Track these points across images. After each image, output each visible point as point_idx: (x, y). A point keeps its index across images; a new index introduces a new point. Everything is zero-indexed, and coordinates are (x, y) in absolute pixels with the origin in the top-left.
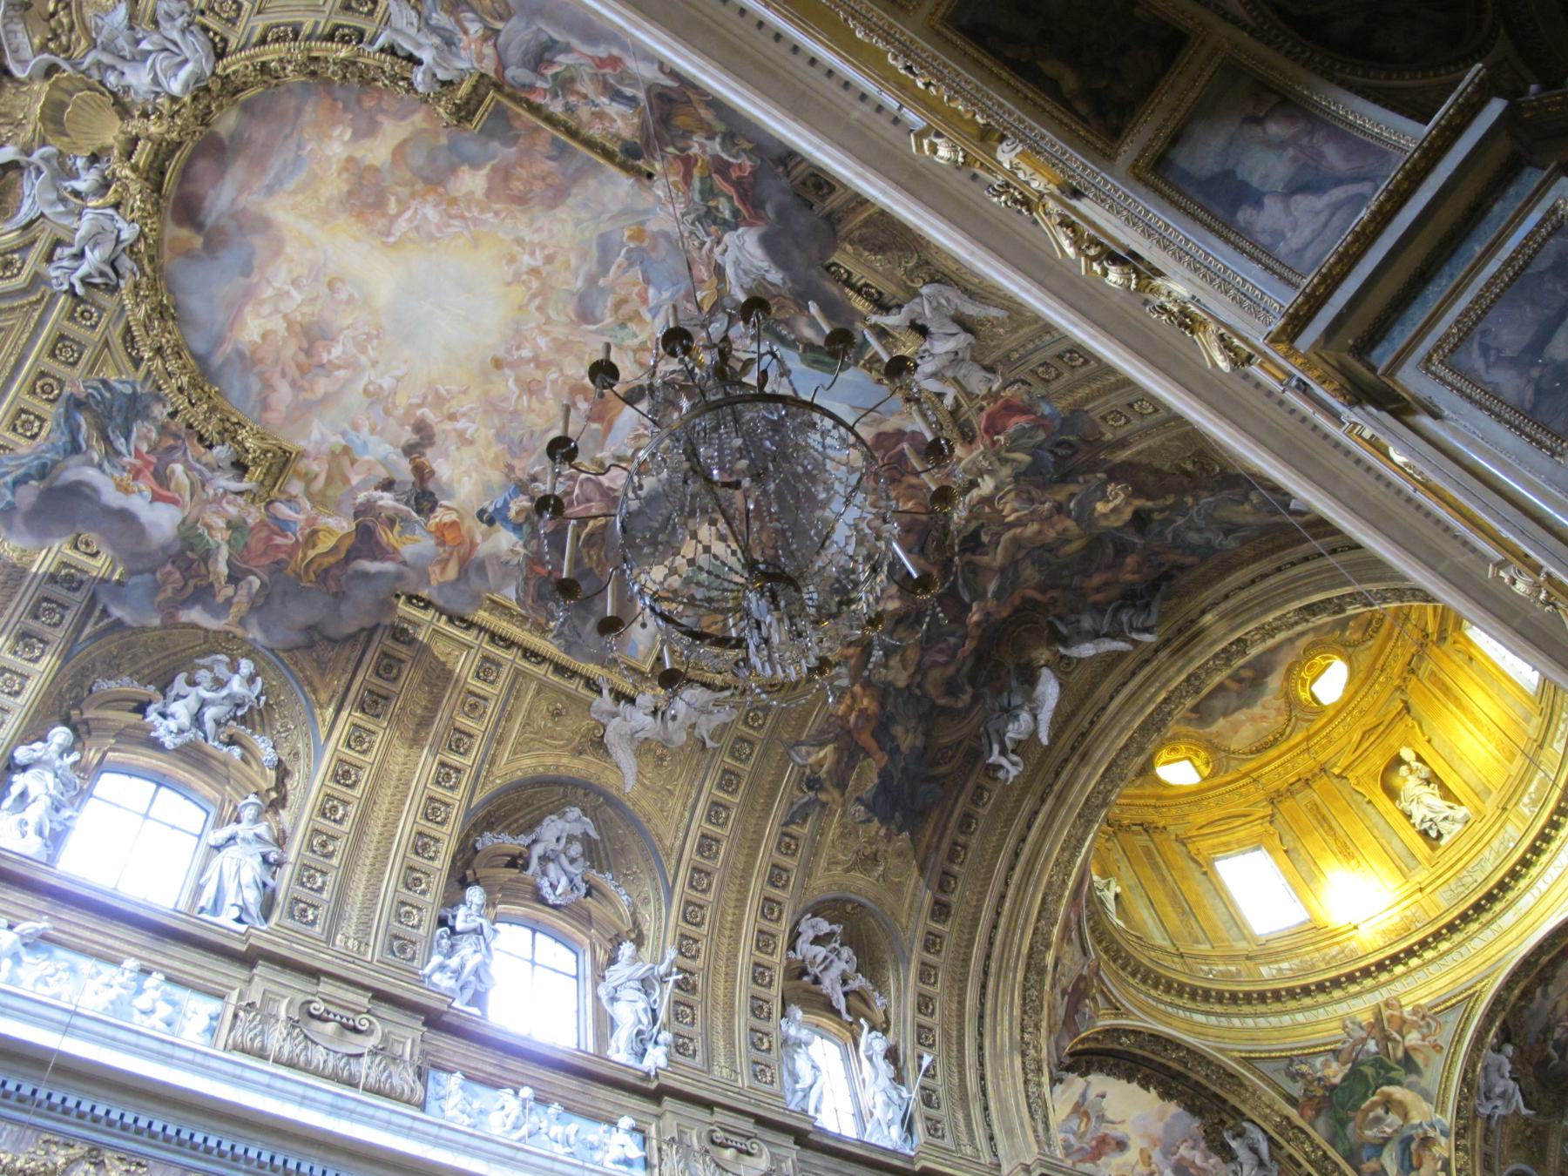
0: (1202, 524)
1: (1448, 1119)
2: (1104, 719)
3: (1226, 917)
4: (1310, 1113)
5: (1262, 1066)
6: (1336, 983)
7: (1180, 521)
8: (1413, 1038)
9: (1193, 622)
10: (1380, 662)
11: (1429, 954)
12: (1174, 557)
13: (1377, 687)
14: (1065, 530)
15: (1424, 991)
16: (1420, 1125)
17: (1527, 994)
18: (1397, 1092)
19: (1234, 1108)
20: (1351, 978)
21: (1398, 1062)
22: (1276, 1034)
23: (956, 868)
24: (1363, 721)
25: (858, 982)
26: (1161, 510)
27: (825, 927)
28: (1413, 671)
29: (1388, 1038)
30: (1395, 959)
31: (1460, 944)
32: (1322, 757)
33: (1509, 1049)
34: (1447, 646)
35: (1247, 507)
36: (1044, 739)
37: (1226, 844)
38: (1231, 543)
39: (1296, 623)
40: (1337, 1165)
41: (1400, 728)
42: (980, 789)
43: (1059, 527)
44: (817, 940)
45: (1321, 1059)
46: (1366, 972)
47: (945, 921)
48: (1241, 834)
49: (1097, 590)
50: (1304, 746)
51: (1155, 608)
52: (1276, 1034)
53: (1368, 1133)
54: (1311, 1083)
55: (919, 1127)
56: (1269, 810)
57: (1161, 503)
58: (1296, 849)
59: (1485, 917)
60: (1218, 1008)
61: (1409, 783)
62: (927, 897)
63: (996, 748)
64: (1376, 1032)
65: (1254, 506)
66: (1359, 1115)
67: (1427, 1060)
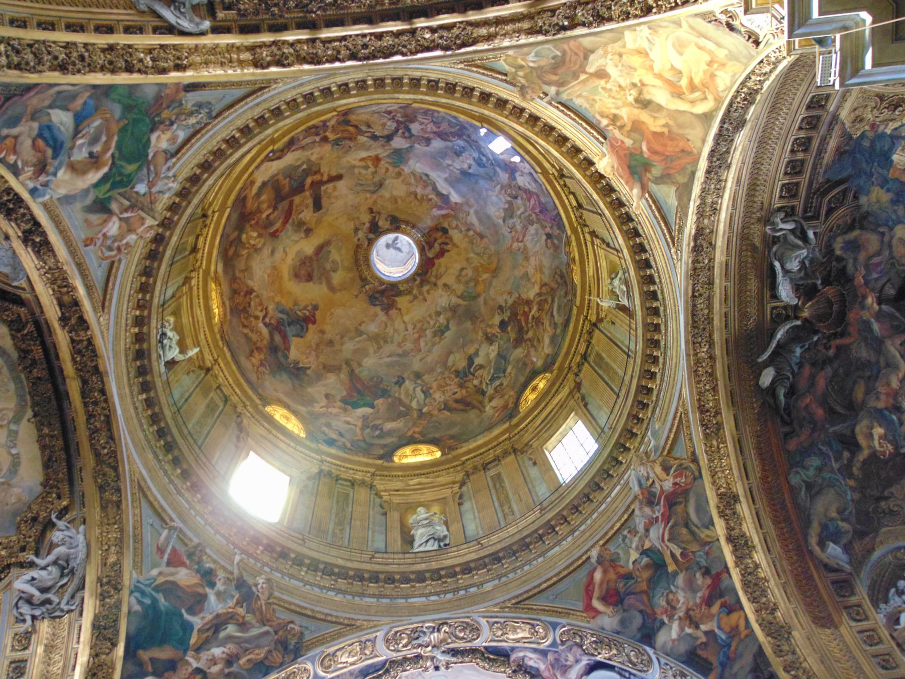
0: (827, 475)
4: (168, 91)
5: (239, 92)
7: (836, 466)
8: (113, 227)
10: (222, 365)
12: (803, 436)
14: (878, 398)
16: (55, 174)
19: (227, 30)
21: (110, 198)
26: (850, 460)
29: (132, 207)
35: (834, 514)
40: (113, 72)
43: (883, 397)
45: (180, 140)
49: (812, 377)
50: (204, 266)
53: (97, 123)
54: (178, 115)
64: (146, 201)
66: (115, 128)
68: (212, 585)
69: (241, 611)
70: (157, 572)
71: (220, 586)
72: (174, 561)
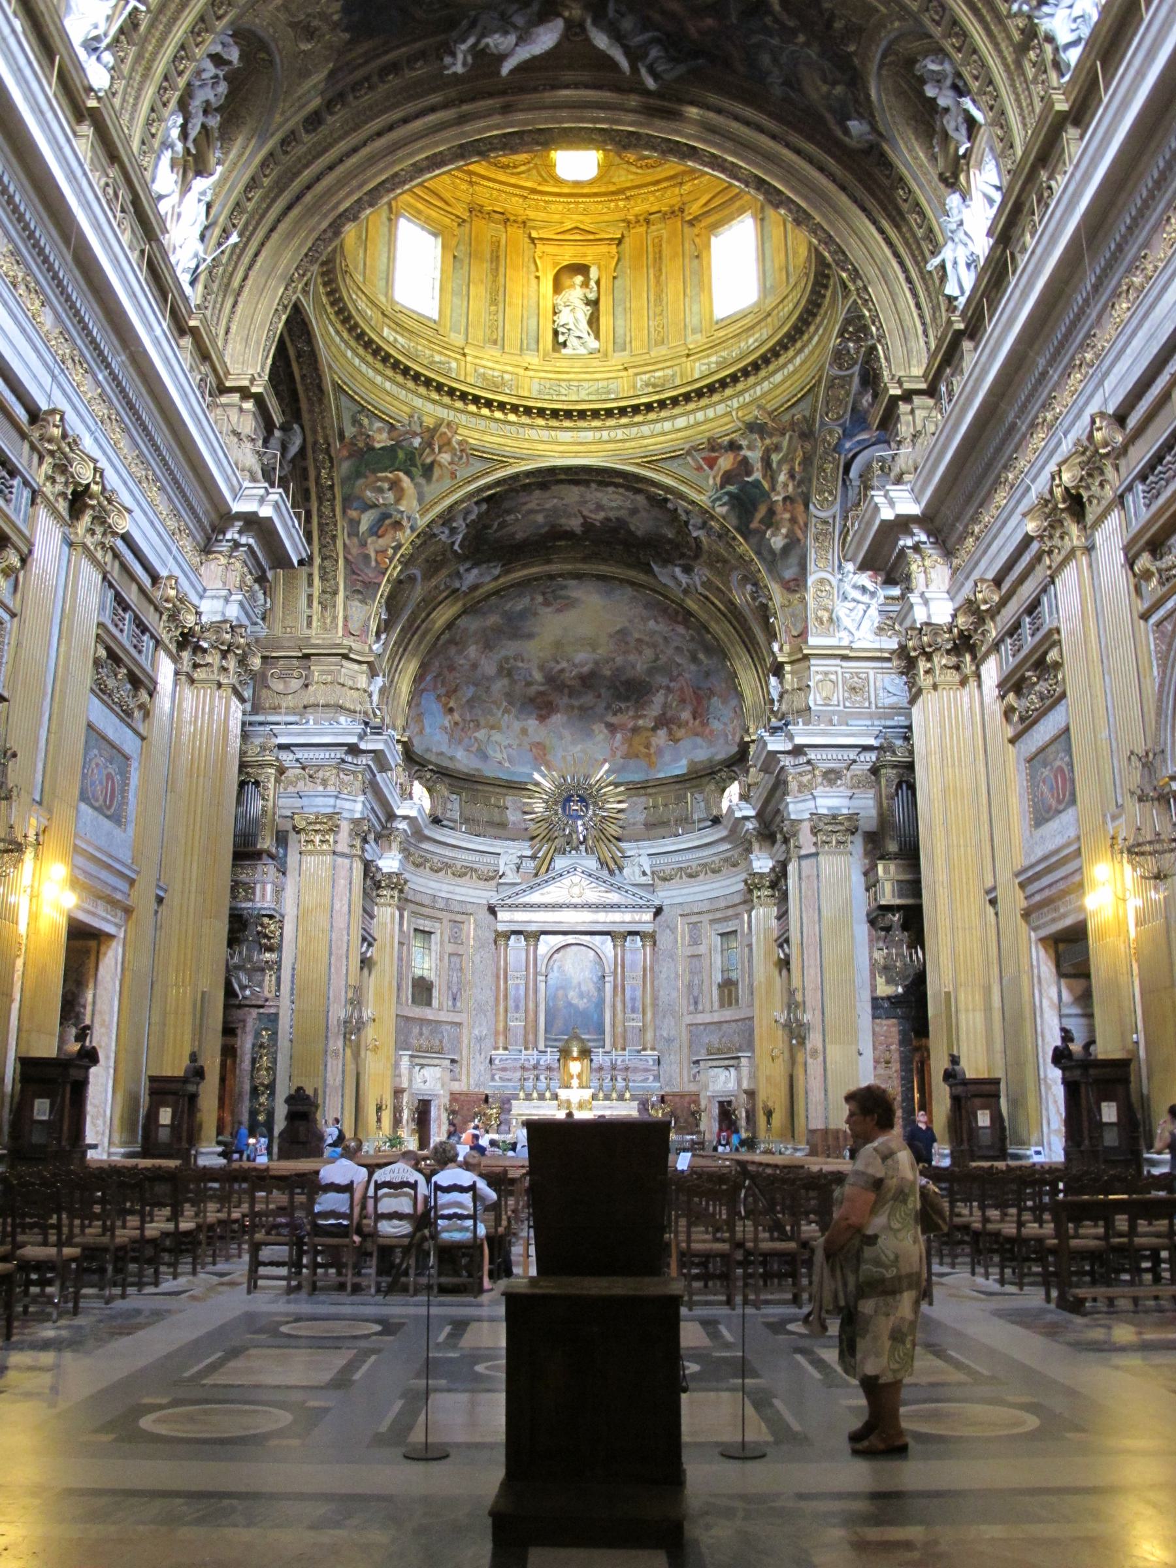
0: (783, 59)
1: (422, 522)
2: (549, 96)
3: (384, 268)
4: (345, 453)
5: (343, 398)
6: (428, 382)
8: (445, 458)
9: (681, 101)
11: (498, 415)
13: (612, 205)
15: (477, 435)
17: (526, 488)
18: (406, 481)
20: (439, 388)
22: (367, 385)
23: (351, 98)
24: (581, 218)
25: (214, 122)
27: (234, 55)
28: (648, 222)
29: (430, 445)
30: (476, 400)
31: (523, 425)
32: (532, 214)
33: (484, 507)
34: (687, 229)
35: (825, 88)
36: (506, 68)
37: (420, 212)
38: (778, 91)
39: (739, 180)
41: (603, 249)
42: (422, 55)
44: (217, 59)
45: (381, 425)
46: (451, 392)
47: (308, 132)
48: (434, 214)
49: (663, 12)
51: (681, 69)
52: (367, 385)
53: (368, 493)
54: (362, 434)
55: (200, 287)
56: (465, 216)
57: (784, 17)
58: (462, 261)
59: (554, 423)
60: (345, 335)
61: (575, 293)
62: (316, 103)
63: (471, 41)
64: (426, 435)
65: (829, 93)
66: (372, 478)
67: (441, 477)
68: (740, 448)
69: (768, 441)
70: (712, 479)
71: (744, 443)
72: (711, 463)
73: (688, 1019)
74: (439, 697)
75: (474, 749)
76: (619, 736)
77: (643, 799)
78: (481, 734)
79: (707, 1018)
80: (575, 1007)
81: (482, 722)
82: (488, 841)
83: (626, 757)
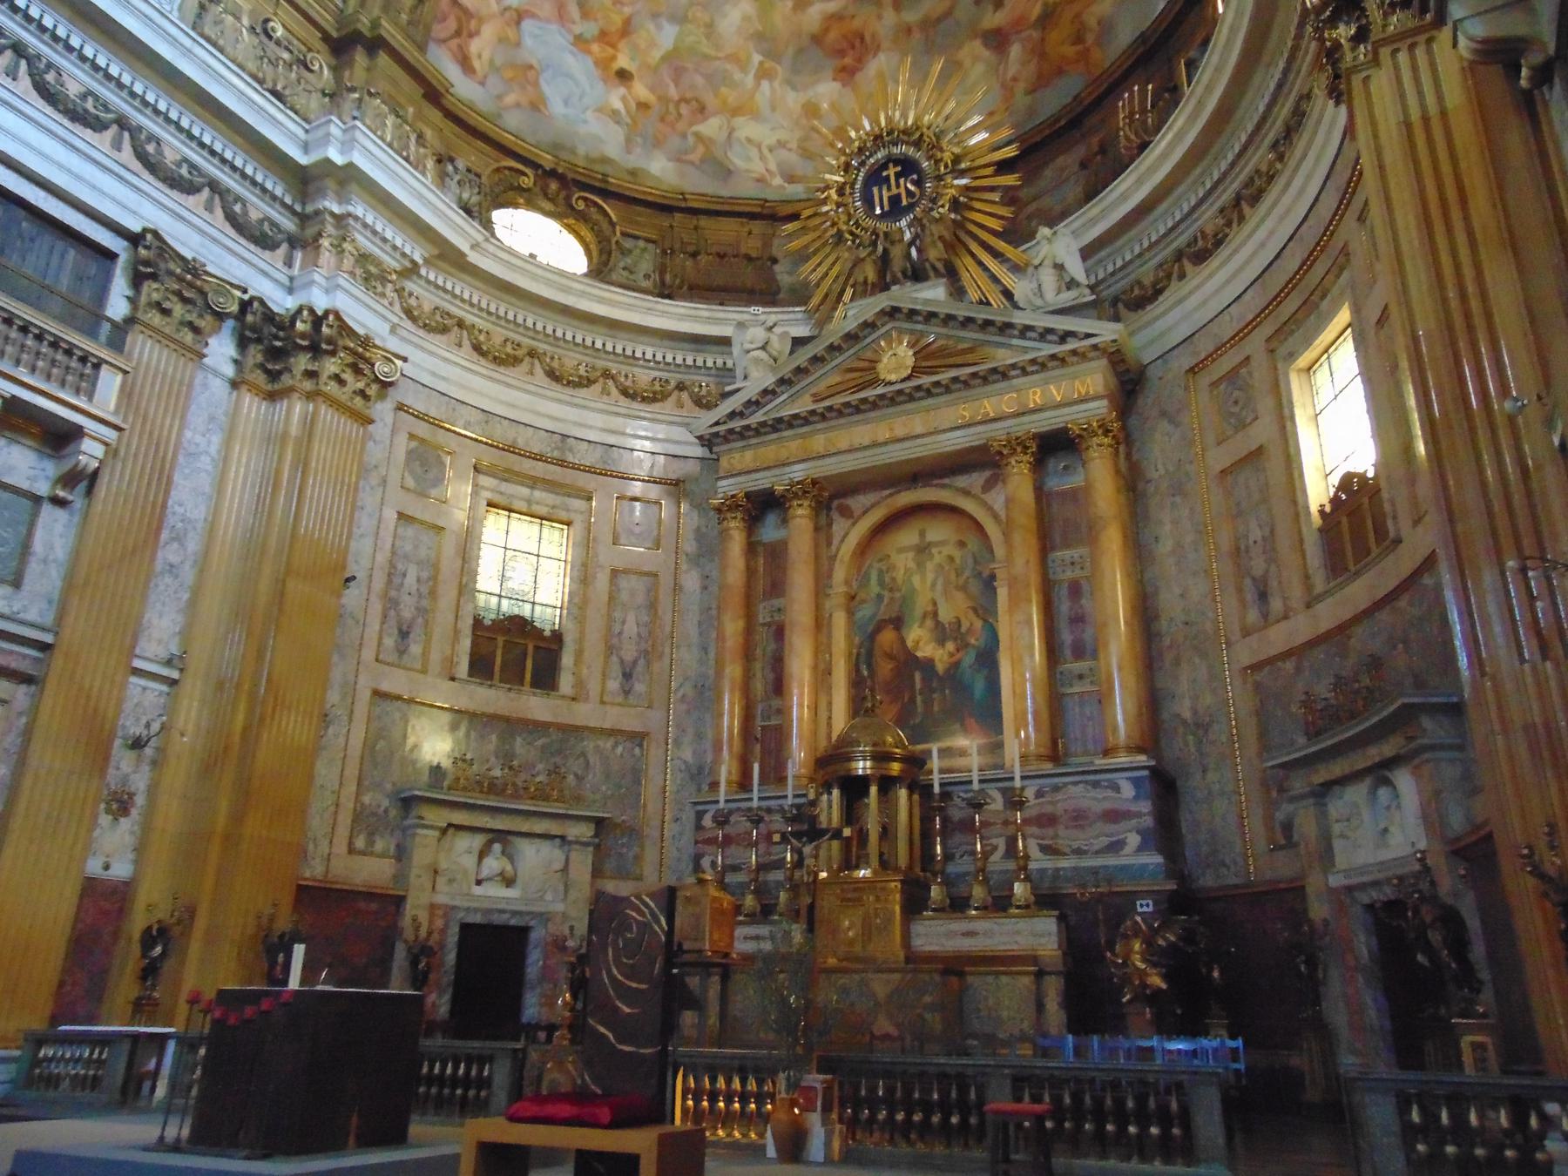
73: (1246, 654)
74: (580, 41)
75: (695, 157)
76: (1015, 51)
77: (1080, 152)
78: (711, 127)
79: (1301, 628)
80: (927, 665)
81: (710, 100)
82: (703, 310)
83: (1040, 83)
